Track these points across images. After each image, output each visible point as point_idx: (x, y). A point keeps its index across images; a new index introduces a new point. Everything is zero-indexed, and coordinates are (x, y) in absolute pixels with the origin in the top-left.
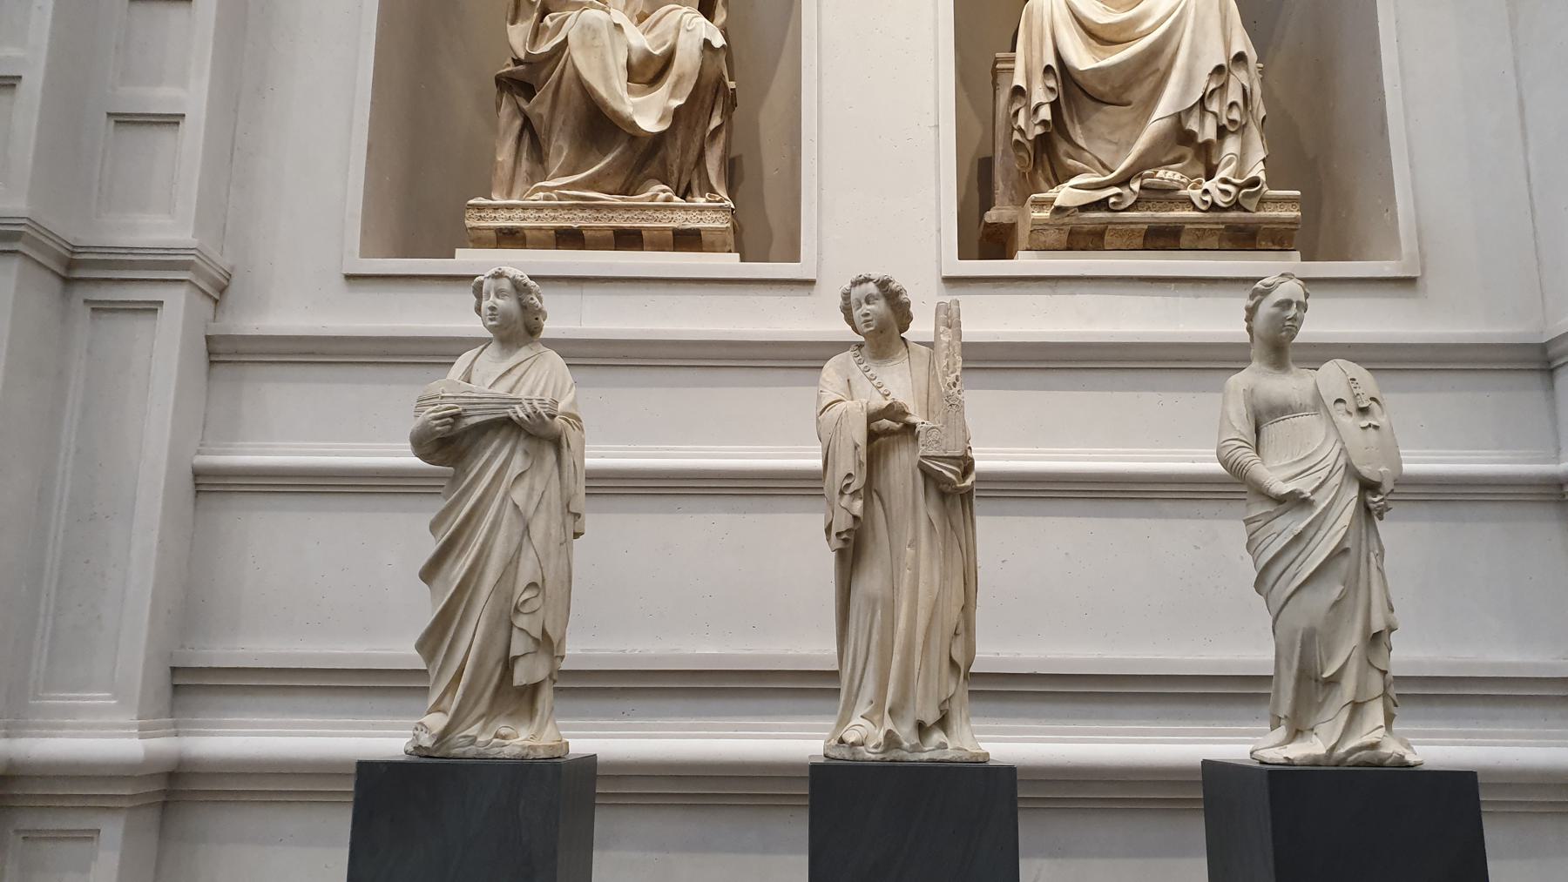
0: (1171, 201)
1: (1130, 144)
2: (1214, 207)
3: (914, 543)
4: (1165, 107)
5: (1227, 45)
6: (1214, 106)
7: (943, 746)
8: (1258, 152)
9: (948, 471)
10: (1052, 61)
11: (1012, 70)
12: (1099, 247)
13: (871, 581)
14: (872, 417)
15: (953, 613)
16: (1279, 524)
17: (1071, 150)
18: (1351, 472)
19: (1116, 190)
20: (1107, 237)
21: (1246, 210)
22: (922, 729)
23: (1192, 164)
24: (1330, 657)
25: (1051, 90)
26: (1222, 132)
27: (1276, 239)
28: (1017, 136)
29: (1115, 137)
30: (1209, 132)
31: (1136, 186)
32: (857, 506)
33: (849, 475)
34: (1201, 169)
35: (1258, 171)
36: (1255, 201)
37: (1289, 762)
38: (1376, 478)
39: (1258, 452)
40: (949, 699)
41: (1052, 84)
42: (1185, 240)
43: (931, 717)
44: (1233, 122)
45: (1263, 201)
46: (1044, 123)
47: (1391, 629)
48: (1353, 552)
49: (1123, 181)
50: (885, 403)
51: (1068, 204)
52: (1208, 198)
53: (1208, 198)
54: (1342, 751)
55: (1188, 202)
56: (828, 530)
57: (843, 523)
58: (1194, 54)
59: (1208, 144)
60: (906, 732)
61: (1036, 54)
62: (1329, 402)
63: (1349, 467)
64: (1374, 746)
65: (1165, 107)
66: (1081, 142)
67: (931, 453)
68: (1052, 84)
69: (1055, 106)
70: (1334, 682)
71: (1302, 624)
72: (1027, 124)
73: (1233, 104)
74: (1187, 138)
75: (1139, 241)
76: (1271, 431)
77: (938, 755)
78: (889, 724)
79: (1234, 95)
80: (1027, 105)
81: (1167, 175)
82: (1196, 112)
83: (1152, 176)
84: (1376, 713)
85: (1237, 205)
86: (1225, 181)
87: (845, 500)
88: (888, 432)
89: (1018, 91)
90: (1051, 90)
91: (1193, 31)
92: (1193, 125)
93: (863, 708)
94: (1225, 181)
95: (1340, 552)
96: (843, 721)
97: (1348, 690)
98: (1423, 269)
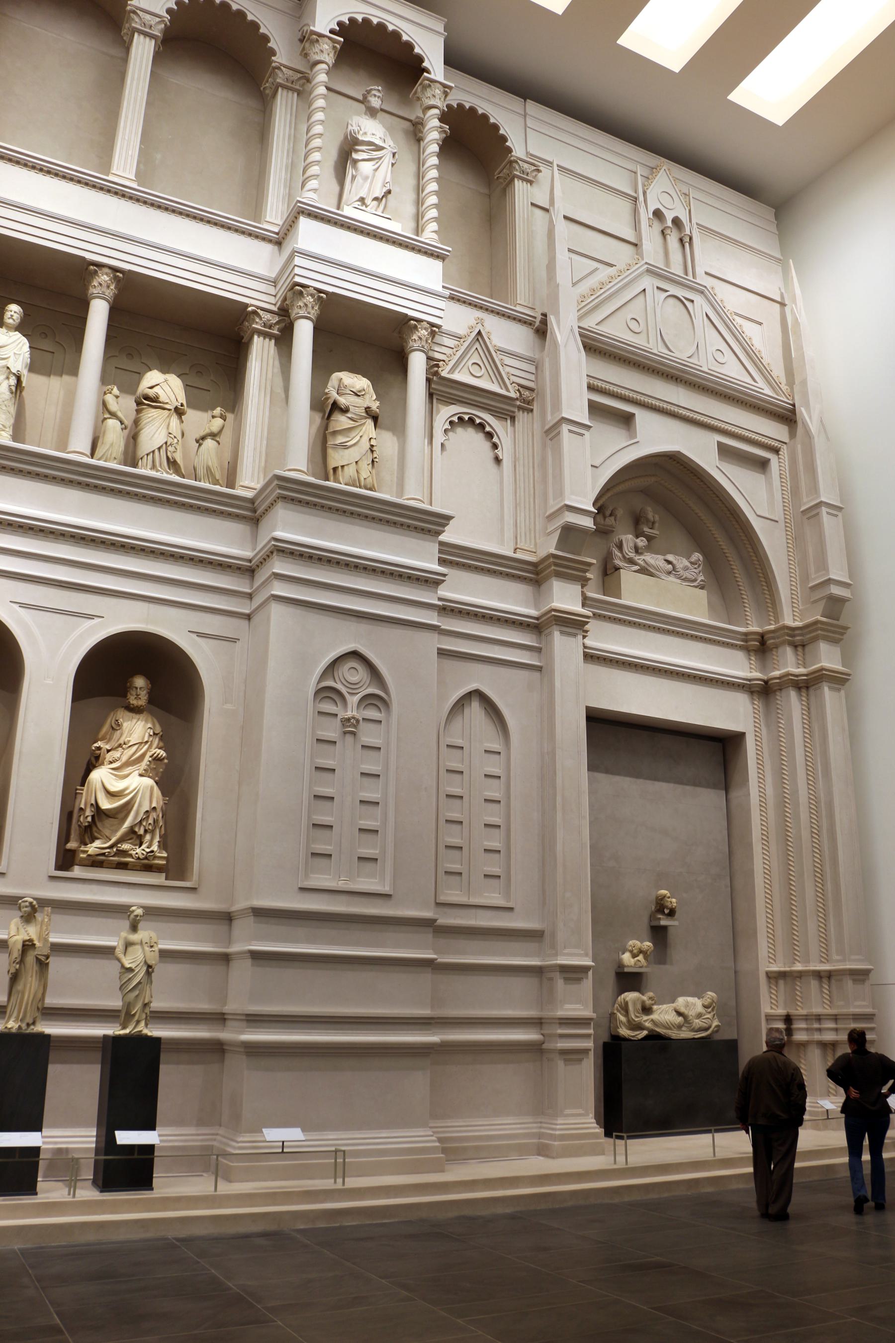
0: (126, 855)
1: (117, 831)
2: (139, 858)
3: (32, 976)
4: (127, 824)
5: (151, 802)
6: (144, 823)
7: (33, 1029)
8: (157, 839)
9: (43, 958)
10: (93, 802)
11: (82, 794)
12: (102, 867)
13: (19, 987)
14: (24, 941)
15: (39, 995)
16: (126, 975)
17: (97, 830)
18: (146, 962)
19: (108, 850)
20: (104, 864)
21: (149, 860)
22: (28, 1025)
23: (135, 840)
24: (134, 1009)
25: (92, 811)
26: (146, 831)
27: (159, 869)
28: (79, 823)
29: (111, 828)
30: (142, 832)
31: (115, 850)
32: (18, 966)
33: (16, 958)
34: (138, 842)
35: (155, 847)
36: (152, 858)
37: (120, 1035)
38: (151, 964)
39: (125, 955)
40: (36, 1017)
41: (93, 810)
42: (129, 867)
43: (31, 1022)
44: (149, 829)
45: (155, 857)
46: (88, 822)
47: (151, 1002)
48: (143, 983)
49: (111, 847)
50: (29, 938)
51: (92, 854)
52: (137, 856)
53: (137, 856)
54: (133, 1032)
55: (131, 856)
56: (9, 972)
57: (13, 970)
58: (140, 805)
59: (141, 835)
60: (24, 1026)
61: (89, 798)
62: (144, 943)
63: (145, 961)
64: (141, 1031)
65: (127, 824)
66: (100, 828)
67: (39, 953)
68: (93, 810)
69: (93, 817)
70: (134, 1015)
71: (128, 1001)
72: (84, 820)
73: (150, 824)
74: (135, 833)
75: (114, 866)
76: (130, 949)
77: (32, 1031)
78: (19, 1024)
79: (151, 821)
80: (84, 814)
81: (125, 846)
82: (139, 824)
83: (120, 847)
84: (143, 1024)
85: (146, 858)
86: (143, 850)
87: (14, 965)
88: (28, 945)
89: (81, 809)
90: (92, 811)
91: (141, 798)
92: (136, 829)
93: (13, 1019)
94: (143, 850)
95: (139, 983)
96: (7, 1022)
97: (136, 1018)
98: (199, 885)
